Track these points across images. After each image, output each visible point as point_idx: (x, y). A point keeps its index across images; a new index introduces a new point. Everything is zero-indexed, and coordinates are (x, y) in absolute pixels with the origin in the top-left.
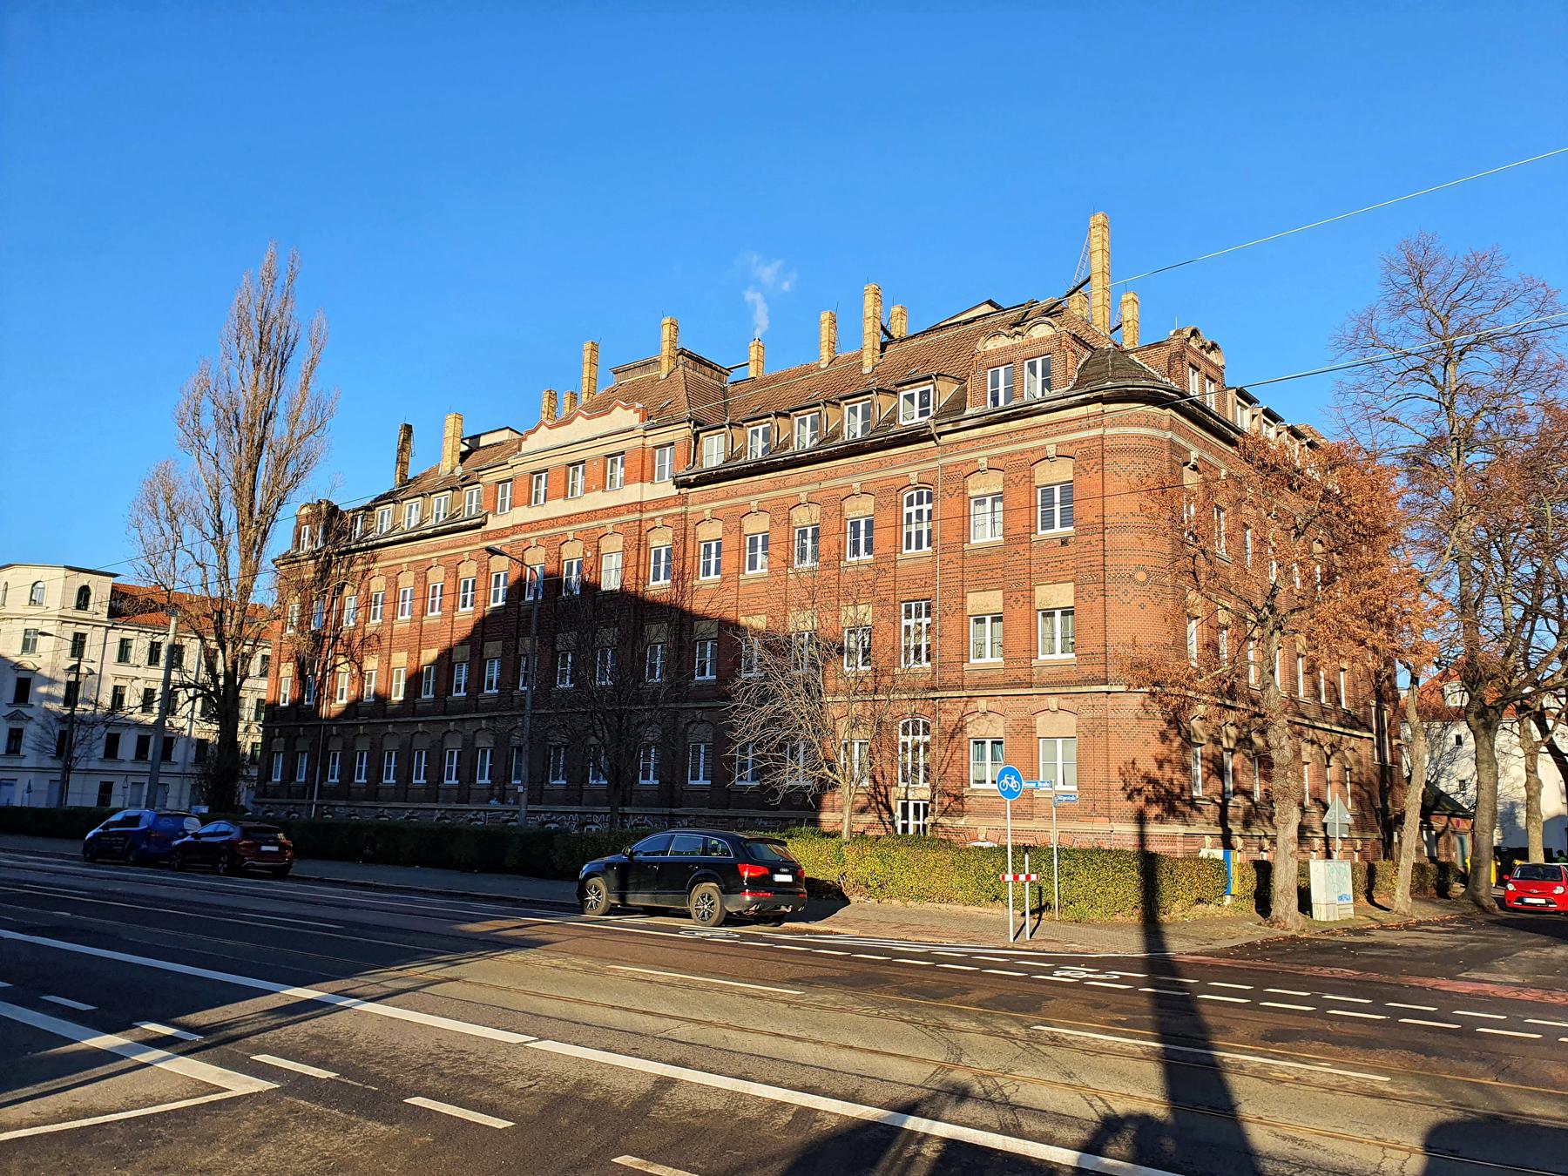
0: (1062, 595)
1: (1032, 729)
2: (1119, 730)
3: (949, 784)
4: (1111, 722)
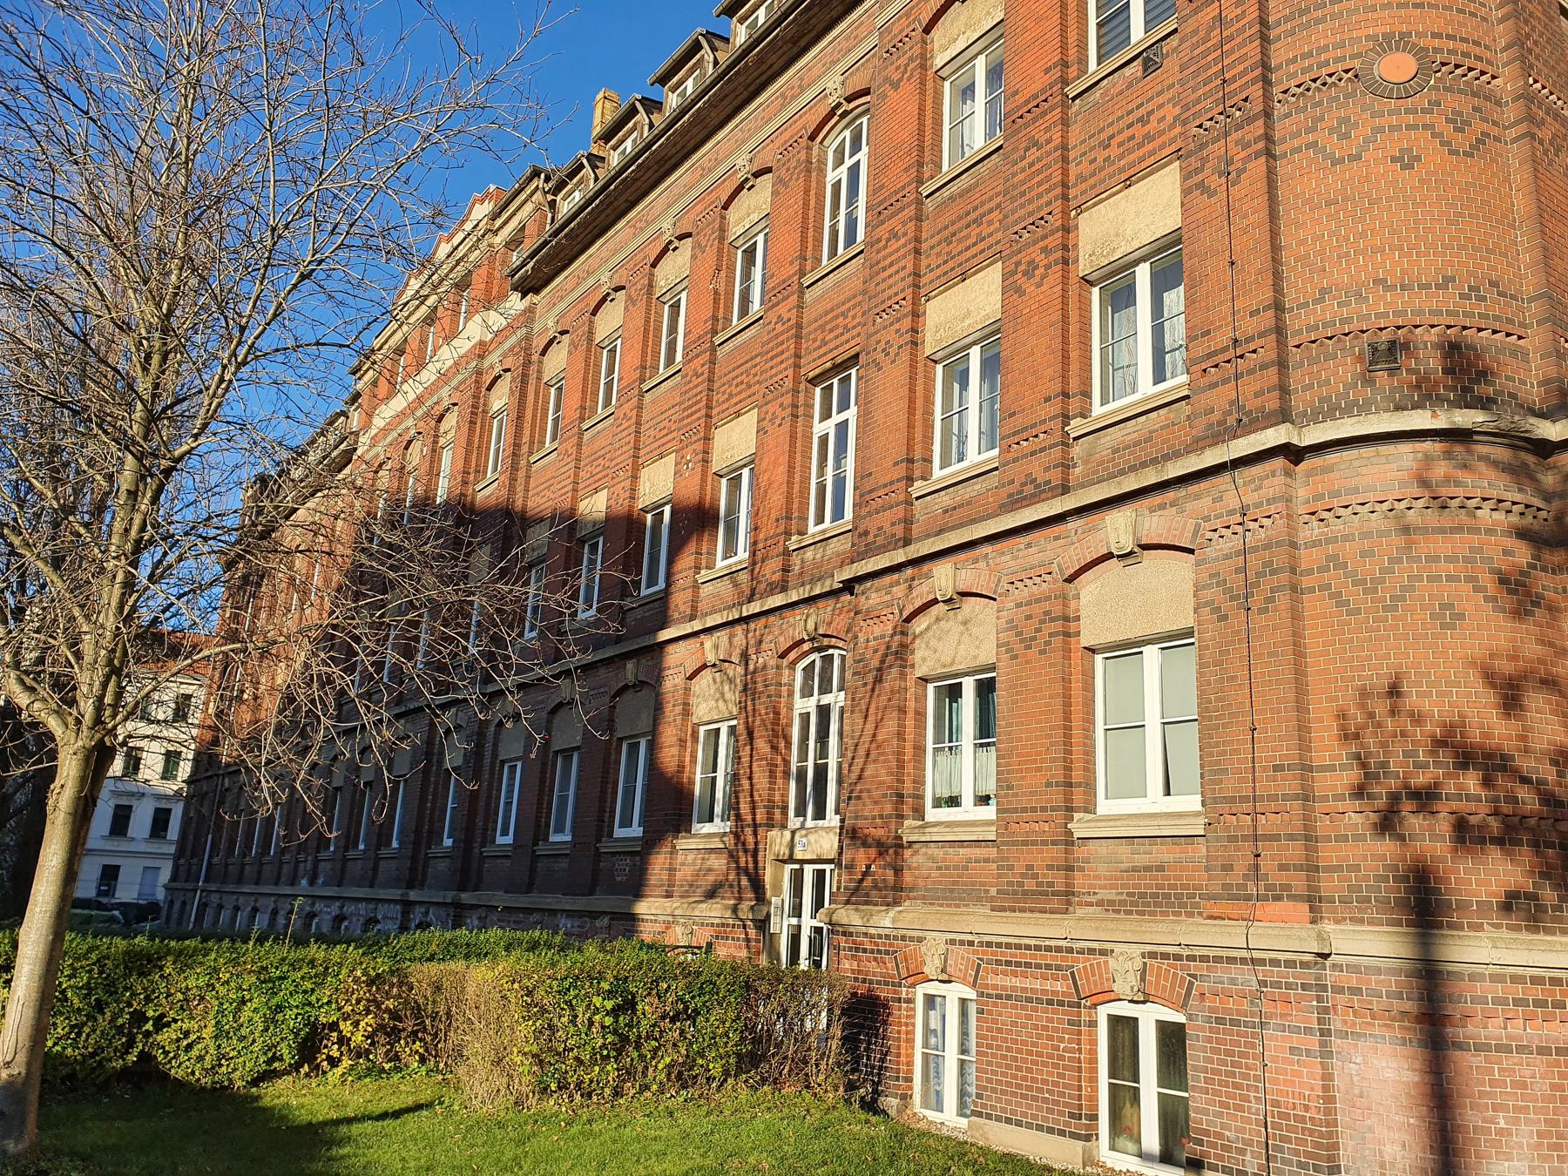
0: (1145, 210)
1: (1067, 624)
2: (1335, 578)
3: (869, 810)
4: (1306, 558)
